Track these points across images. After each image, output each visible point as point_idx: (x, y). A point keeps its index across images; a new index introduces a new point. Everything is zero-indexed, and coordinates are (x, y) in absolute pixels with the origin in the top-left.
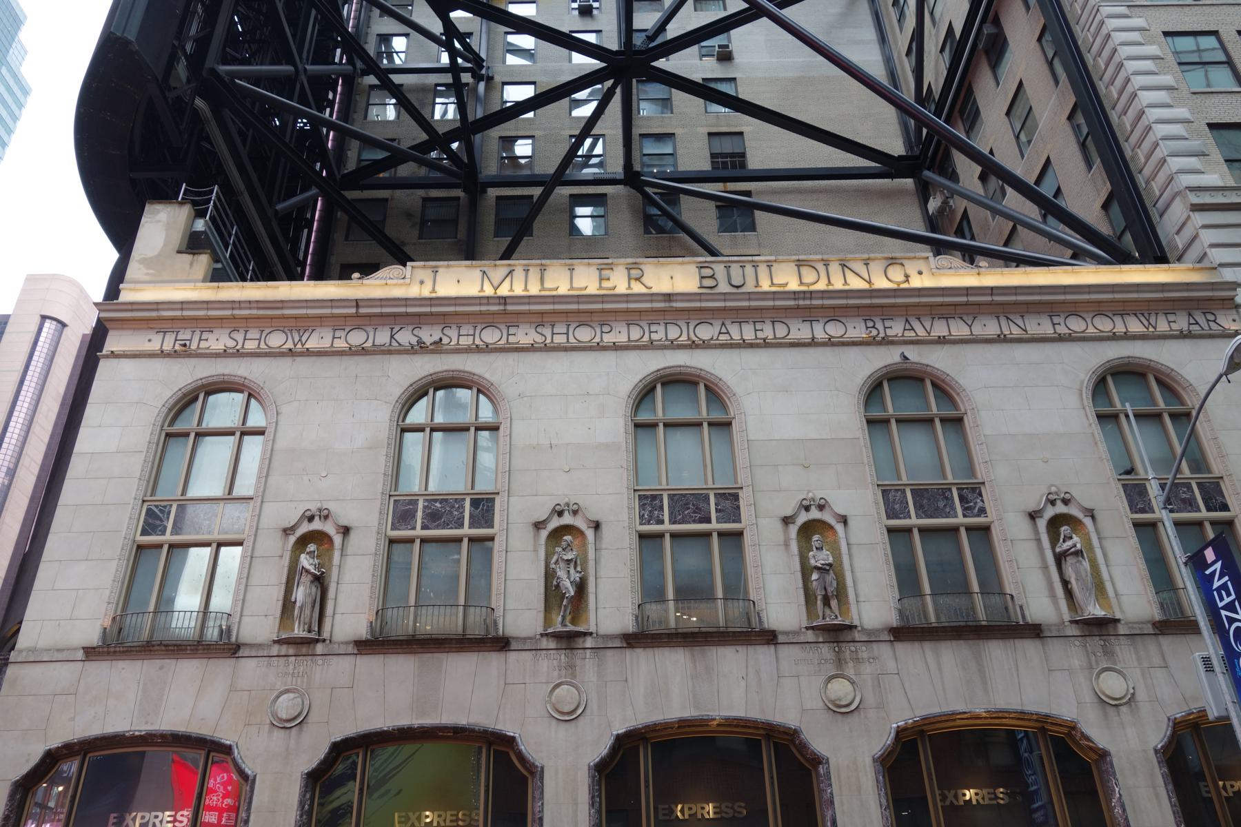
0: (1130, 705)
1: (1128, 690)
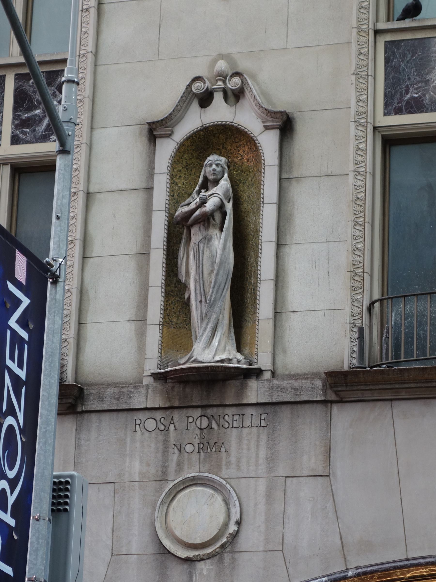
0: (221, 561)
1: (226, 525)
